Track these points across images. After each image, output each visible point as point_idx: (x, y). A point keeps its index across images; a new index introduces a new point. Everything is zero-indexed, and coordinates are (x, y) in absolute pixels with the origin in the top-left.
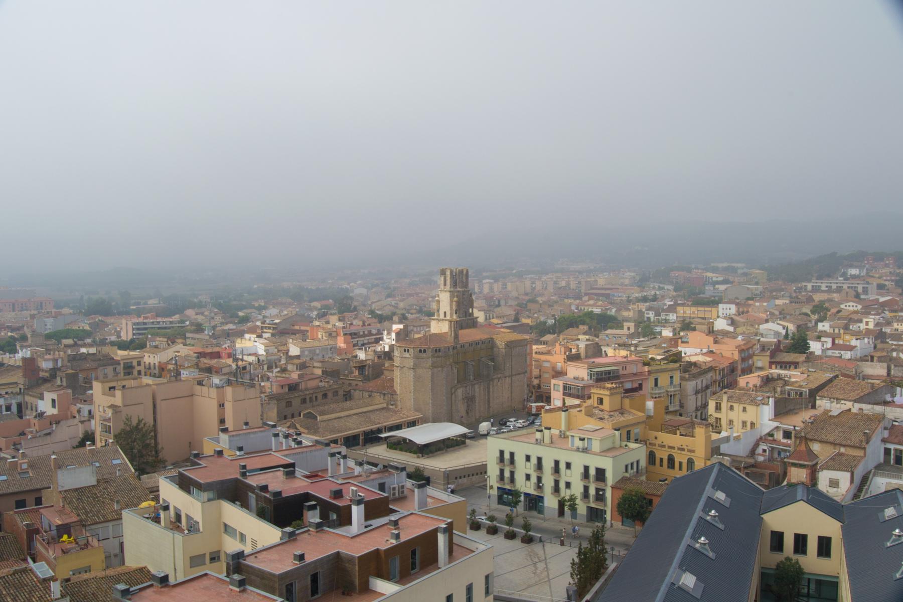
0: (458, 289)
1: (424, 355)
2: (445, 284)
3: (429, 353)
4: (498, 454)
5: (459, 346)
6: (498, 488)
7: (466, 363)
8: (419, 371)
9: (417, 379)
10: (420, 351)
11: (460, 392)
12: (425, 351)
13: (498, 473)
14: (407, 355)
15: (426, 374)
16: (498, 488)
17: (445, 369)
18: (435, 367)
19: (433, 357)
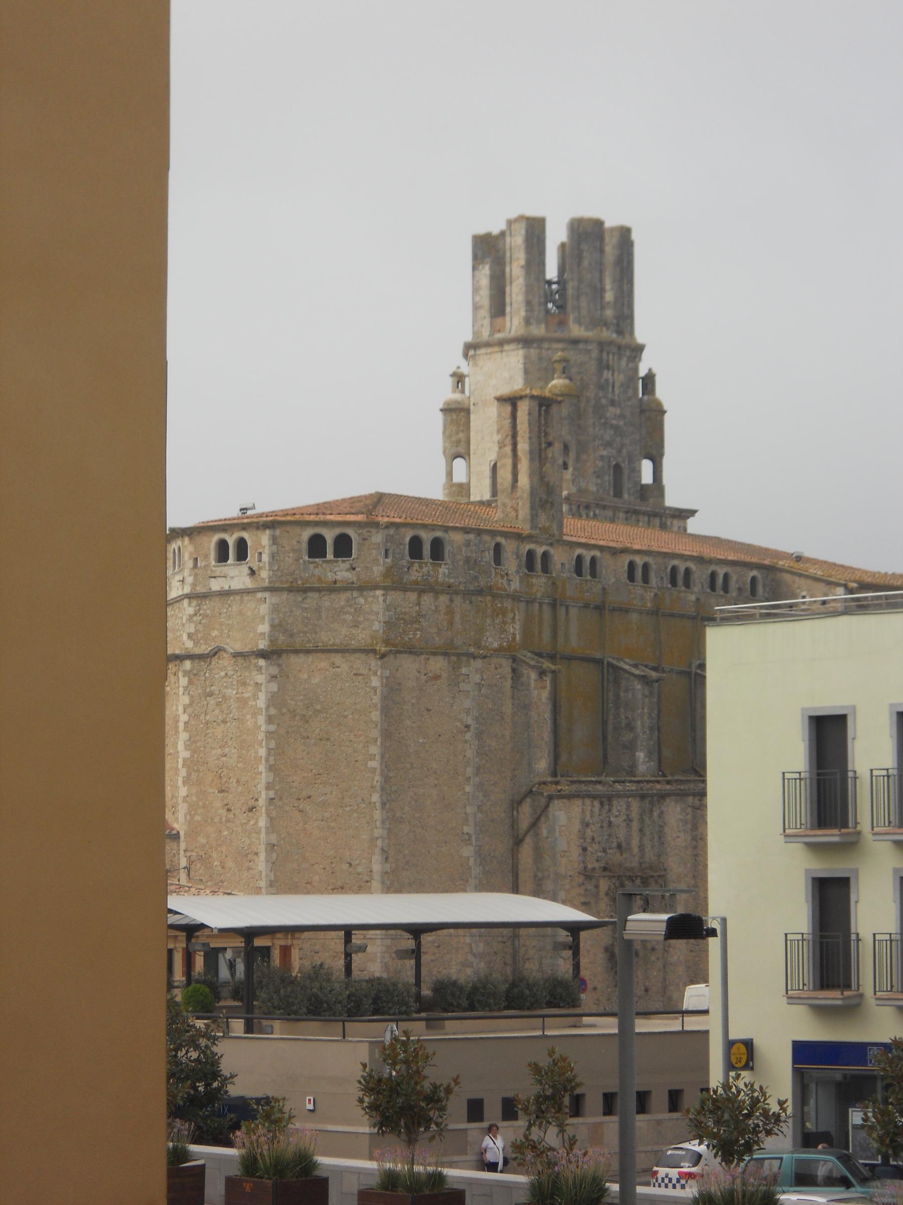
0: (576, 331)
1: (341, 571)
2: (498, 307)
3: (371, 559)
4: (796, 755)
5: (560, 558)
6: (804, 1053)
7: (610, 674)
8: (311, 672)
9: (292, 719)
10: (316, 547)
11: (566, 820)
12: (343, 546)
13: (799, 918)
14: (236, 576)
15: (354, 690)
16: (804, 1053)
17: (472, 670)
18: (411, 651)
19: (395, 583)
